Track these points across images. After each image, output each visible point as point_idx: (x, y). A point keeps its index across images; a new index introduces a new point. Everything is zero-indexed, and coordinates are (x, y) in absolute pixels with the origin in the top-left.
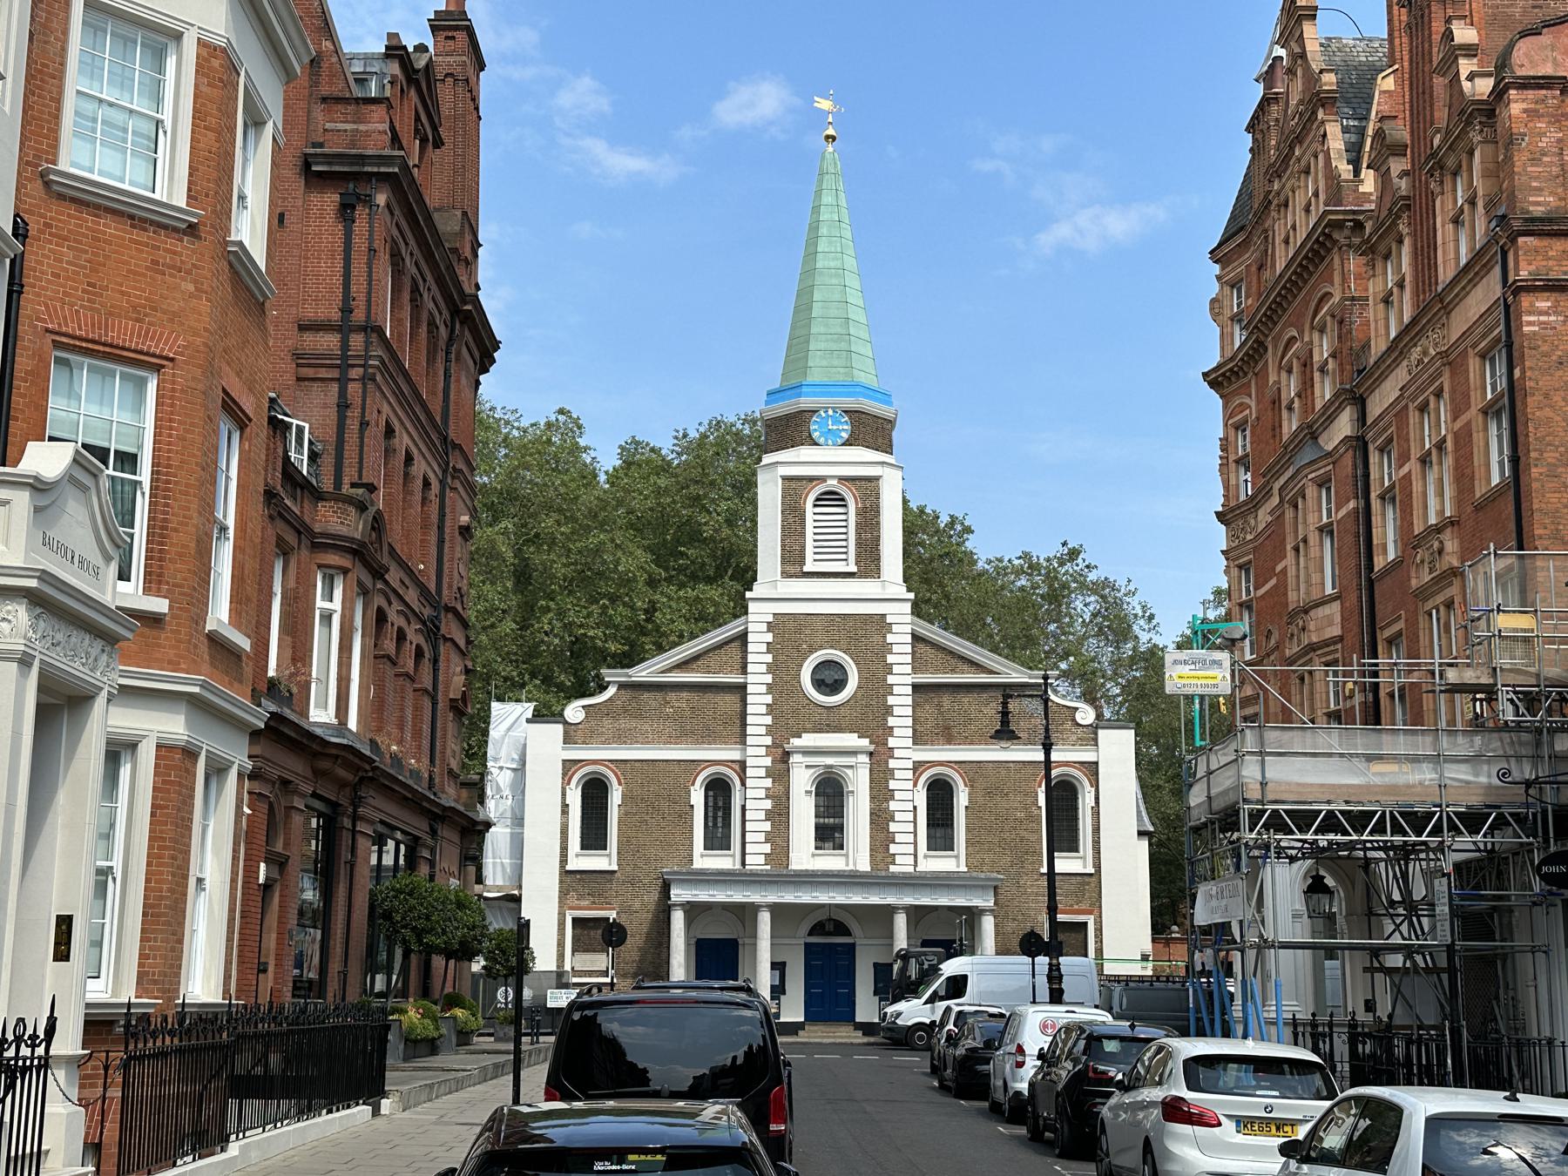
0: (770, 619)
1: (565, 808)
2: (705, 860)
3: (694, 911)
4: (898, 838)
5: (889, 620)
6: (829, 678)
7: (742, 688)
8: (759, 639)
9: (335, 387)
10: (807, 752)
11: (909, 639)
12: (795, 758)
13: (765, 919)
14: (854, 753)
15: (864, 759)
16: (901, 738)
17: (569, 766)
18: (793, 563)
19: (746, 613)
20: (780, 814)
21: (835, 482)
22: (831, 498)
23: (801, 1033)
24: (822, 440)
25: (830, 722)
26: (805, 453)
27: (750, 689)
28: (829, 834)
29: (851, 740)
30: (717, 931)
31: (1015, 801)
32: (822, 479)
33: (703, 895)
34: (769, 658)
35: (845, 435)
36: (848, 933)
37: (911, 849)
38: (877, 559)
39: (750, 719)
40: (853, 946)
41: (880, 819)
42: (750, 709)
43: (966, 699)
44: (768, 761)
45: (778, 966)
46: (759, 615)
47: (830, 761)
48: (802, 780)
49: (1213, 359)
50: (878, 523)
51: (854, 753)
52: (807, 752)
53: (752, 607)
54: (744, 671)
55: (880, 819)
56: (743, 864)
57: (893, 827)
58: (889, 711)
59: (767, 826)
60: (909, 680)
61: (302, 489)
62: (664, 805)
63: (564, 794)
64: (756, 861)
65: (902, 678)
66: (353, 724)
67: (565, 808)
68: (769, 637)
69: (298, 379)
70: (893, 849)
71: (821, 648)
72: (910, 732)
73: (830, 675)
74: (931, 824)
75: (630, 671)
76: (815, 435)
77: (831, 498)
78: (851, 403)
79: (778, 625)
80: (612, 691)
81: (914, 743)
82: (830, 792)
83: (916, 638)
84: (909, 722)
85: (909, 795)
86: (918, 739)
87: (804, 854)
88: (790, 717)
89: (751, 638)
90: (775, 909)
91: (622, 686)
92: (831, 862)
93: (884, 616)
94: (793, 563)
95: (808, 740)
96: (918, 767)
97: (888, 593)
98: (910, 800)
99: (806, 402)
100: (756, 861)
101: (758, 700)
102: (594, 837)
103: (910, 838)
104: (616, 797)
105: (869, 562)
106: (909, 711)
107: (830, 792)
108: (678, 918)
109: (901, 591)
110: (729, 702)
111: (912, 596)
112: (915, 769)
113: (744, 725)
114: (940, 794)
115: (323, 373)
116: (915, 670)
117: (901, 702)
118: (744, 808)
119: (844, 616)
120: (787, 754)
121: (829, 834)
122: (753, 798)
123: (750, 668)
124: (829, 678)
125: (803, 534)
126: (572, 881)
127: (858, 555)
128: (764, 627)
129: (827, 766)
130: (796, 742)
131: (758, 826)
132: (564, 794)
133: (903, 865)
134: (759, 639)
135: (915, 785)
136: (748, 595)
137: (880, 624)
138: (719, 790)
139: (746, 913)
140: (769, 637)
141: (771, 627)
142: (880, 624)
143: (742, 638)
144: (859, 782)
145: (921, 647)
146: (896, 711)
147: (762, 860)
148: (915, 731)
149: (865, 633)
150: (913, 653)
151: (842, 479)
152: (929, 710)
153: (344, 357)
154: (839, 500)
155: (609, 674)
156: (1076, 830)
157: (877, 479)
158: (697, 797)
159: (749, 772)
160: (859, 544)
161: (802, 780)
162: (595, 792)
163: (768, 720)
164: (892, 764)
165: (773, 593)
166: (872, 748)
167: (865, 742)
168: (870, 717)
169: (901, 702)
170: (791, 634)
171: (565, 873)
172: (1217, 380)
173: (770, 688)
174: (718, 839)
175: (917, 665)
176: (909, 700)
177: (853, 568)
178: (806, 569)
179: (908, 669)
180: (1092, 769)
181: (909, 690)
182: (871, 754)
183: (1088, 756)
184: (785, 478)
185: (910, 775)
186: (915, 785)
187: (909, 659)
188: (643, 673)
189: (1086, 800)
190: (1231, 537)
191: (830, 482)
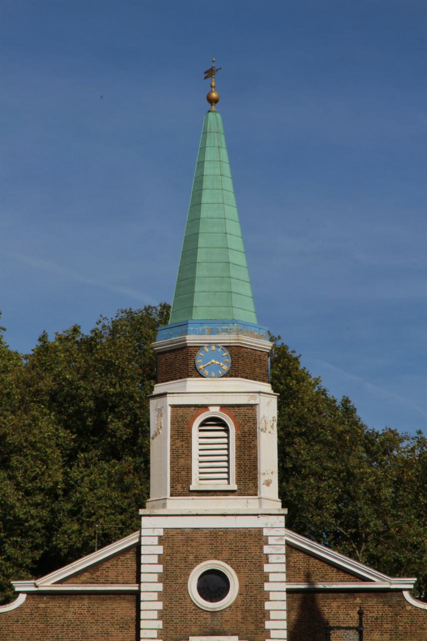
0: (161, 533)
5: (266, 532)
6: (214, 586)
8: (151, 552)
21: (217, 409)
24: (206, 372)
26: (192, 384)
27: (143, 596)
32: (205, 407)
35: (226, 368)
39: (143, 624)
42: (143, 615)
50: (255, 447)
53: (145, 521)
54: (138, 581)
58: (266, 615)
68: (160, 550)
71: (206, 558)
75: (38, 582)
78: (230, 339)
80: (22, 598)
83: (291, 547)
89: (144, 550)
91: (29, 593)
93: (260, 530)
94: (181, 485)
97: (263, 511)
105: (248, 481)
109: (276, 505)
111: (285, 511)
113: (138, 629)
116: (288, 581)
119: (226, 531)
123: (143, 578)
124: (214, 586)
125: (189, 456)
128: (155, 541)
134: (151, 552)
136: (141, 512)
137: (257, 537)
140: (160, 550)
141: (161, 540)
142: (257, 537)
143: (137, 549)
145: (296, 556)
146: (273, 615)
149: (246, 546)
150: (288, 563)
151: (223, 407)
155: (22, 586)
157: (252, 407)
160: (239, 466)
170: (180, 547)
173: (162, 596)
175: (291, 572)
177: (233, 486)
178: (192, 488)
179: (283, 577)
181: (284, 596)
184: (173, 406)
187: (283, 568)
188: (47, 583)
191: (212, 409)
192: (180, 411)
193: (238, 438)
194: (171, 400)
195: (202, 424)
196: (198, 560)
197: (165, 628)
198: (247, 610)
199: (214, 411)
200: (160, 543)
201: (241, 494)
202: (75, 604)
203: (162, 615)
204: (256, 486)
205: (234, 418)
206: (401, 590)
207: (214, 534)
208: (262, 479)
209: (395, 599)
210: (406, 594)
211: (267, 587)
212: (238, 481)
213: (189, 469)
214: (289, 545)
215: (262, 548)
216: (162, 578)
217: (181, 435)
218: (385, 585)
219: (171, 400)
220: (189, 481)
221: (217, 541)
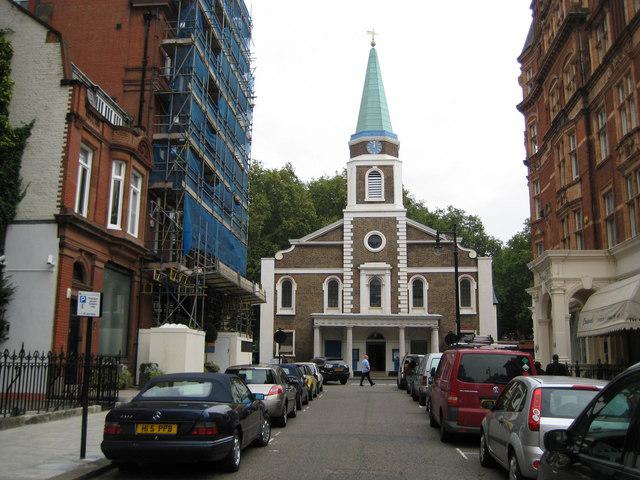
1: (276, 291)
2: (328, 312)
3: (323, 329)
7: (341, 247)
9: (139, 94)
12: (362, 272)
13: (350, 333)
15: (388, 272)
17: (277, 276)
18: (360, 199)
19: (342, 217)
20: (356, 293)
22: (375, 174)
25: (375, 258)
26: (364, 157)
28: (375, 300)
29: (383, 265)
30: (332, 338)
33: (326, 323)
36: (382, 337)
41: (395, 294)
45: (356, 352)
47: (375, 273)
48: (364, 281)
49: (520, 99)
54: (342, 239)
55: (395, 294)
58: (398, 254)
59: (352, 298)
61: (103, 122)
64: (348, 312)
66: (85, 215)
67: (276, 291)
69: (125, 91)
73: (374, 241)
74: (415, 297)
77: (375, 174)
79: (355, 222)
80: (293, 248)
83: (408, 227)
87: (365, 308)
88: (360, 256)
90: (355, 329)
91: (296, 246)
92: (376, 312)
98: (406, 288)
100: (348, 312)
101: (348, 250)
102: (286, 303)
104: (295, 287)
108: (317, 334)
109: (402, 208)
110: (335, 252)
114: (418, 285)
115: (133, 88)
117: (402, 250)
119: (380, 218)
121: (375, 300)
122: (346, 287)
126: (278, 318)
127: (385, 194)
129: (375, 276)
130: (362, 266)
131: (348, 298)
133: (403, 313)
137: (394, 221)
139: (342, 330)
142: (394, 221)
143: (341, 227)
149: (389, 225)
151: (379, 167)
153: (143, 81)
155: (293, 242)
156: (470, 298)
157: (391, 167)
158: (325, 287)
161: (364, 281)
162: (287, 287)
163: (352, 258)
164: (399, 274)
168: (391, 255)
169: (402, 250)
170: (361, 225)
171: (277, 317)
172: (522, 108)
174: (333, 303)
175: (409, 236)
180: (476, 275)
183: (473, 270)
188: (304, 241)
189: (473, 287)
190: (530, 170)
199: (375, 168)
207: (375, 219)
208: (396, 197)
214: (407, 225)
216: (353, 238)
221: (377, 222)
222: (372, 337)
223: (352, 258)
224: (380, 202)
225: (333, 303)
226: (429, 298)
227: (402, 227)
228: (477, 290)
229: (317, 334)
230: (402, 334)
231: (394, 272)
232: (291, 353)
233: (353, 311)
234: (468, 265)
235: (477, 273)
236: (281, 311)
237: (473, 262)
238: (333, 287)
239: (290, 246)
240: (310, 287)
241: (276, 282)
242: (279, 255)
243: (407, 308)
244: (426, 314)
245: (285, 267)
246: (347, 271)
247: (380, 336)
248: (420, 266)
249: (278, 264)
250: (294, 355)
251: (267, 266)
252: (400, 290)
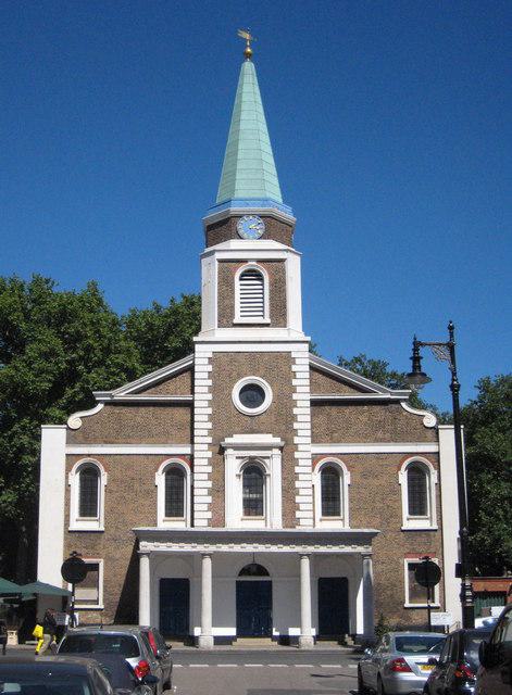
1: (68, 487)
2: (164, 524)
3: (155, 557)
4: (302, 507)
6: (253, 394)
7: (190, 405)
10: (237, 447)
11: (307, 368)
12: (229, 452)
13: (207, 564)
14: (269, 448)
16: (303, 438)
20: (218, 491)
23: (234, 643)
24: (245, 235)
26: (234, 244)
27: (196, 404)
28: (253, 506)
31: (383, 481)
34: (210, 382)
37: (310, 514)
38: (284, 315)
39: (196, 425)
40: (269, 585)
41: (289, 492)
42: (196, 418)
43: (348, 410)
44: (210, 454)
46: (202, 353)
48: (233, 466)
50: (284, 290)
51: (269, 448)
52: (237, 447)
54: (193, 393)
55: (289, 492)
56: (192, 525)
57: (298, 499)
58: (294, 418)
60: (309, 397)
62: (137, 486)
63: (67, 478)
65: (303, 396)
67: (68, 487)
68: (210, 368)
70: (298, 514)
71: (246, 375)
72: (309, 433)
76: (241, 232)
79: (214, 360)
80: (100, 407)
81: (313, 442)
82: (254, 475)
83: (313, 368)
84: (308, 426)
85: (308, 477)
86: (315, 439)
88: (224, 423)
89: (196, 369)
91: (107, 403)
92: (255, 525)
94: (226, 319)
95: (238, 439)
96: (315, 458)
98: (310, 482)
99: (234, 209)
100: (201, 524)
101: (203, 411)
102: (88, 508)
103: (310, 507)
105: (279, 316)
106: (308, 418)
107: (254, 475)
112: (313, 459)
113: (192, 429)
114: (330, 475)
117: (303, 411)
118: (192, 487)
120: (222, 450)
121: (253, 506)
124: (253, 394)
125: (232, 297)
128: (206, 361)
129: (251, 458)
130: (228, 440)
131: (203, 499)
132: (67, 478)
133: (305, 526)
134: (203, 369)
135: (313, 470)
136: (195, 339)
138: (176, 475)
139: (194, 560)
140: (210, 368)
142: (288, 358)
143: (191, 369)
144: (274, 468)
147: (205, 523)
148: (312, 433)
149: (278, 366)
152: (322, 418)
154: (259, 277)
155: (100, 395)
157: (282, 261)
158: (160, 480)
159: (196, 462)
160: (272, 305)
162: (89, 475)
163: (210, 425)
164: (297, 455)
165: (212, 340)
166: (283, 444)
167: (277, 440)
168: (282, 421)
169: (303, 411)
170: (225, 367)
174: (175, 507)
175: (314, 386)
176: (308, 411)
177: (268, 321)
178: (235, 321)
182: (281, 449)
183: (432, 448)
184: (220, 261)
185: (309, 462)
186: (313, 470)
187: (307, 382)
188: (121, 394)
192: (226, 265)
193: (271, 284)
194: (218, 256)
195: (242, 275)
196: (240, 376)
197: (214, 428)
198: (279, 414)
199: (252, 265)
200: (209, 363)
201: (273, 326)
202: (143, 410)
203: (211, 418)
204: (285, 321)
205: (268, 269)
206: (397, 402)
209: (394, 406)
210: (403, 405)
211: (295, 396)
212: (271, 317)
213: (232, 307)
215: (290, 367)
216: (212, 389)
217: (226, 283)
218: (388, 396)
219: (218, 256)
220: (232, 315)
221: (254, 361)
222: (244, 572)
223: (210, 397)
224: (267, 325)
225: (175, 507)
226: (351, 500)
227: (301, 367)
228: (439, 485)
229: (145, 564)
230: (306, 564)
231: (288, 450)
232: (97, 602)
233: (211, 522)
234: (421, 439)
235: (438, 453)
236: (78, 524)
237: (430, 434)
238: (176, 475)
239: (93, 404)
240: (133, 476)
241: (68, 470)
242: (75, 421)
243: (311, 518)
244: (347, 529)
245: (87, 441)
246: (203, 453)
247: (261, 571)
248: (333, 441)
249: (73, 437)
250: (101, 605)
251: (54, 443)
252: (298, 484)
